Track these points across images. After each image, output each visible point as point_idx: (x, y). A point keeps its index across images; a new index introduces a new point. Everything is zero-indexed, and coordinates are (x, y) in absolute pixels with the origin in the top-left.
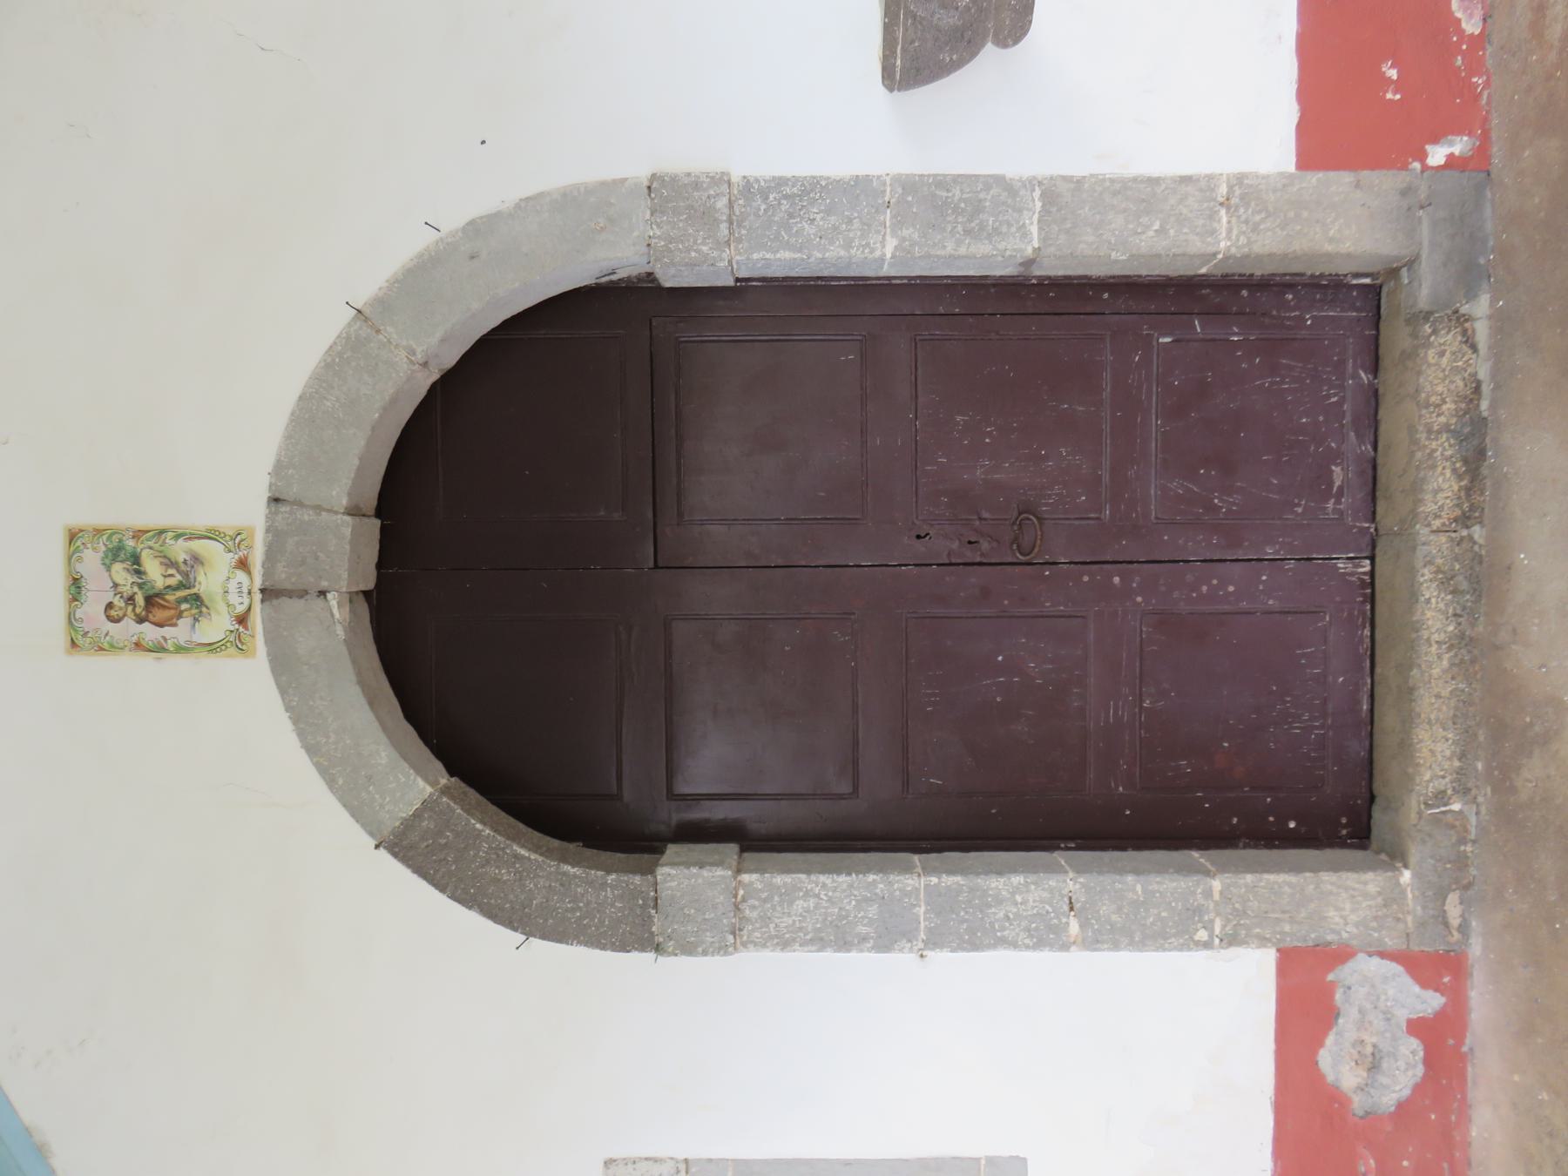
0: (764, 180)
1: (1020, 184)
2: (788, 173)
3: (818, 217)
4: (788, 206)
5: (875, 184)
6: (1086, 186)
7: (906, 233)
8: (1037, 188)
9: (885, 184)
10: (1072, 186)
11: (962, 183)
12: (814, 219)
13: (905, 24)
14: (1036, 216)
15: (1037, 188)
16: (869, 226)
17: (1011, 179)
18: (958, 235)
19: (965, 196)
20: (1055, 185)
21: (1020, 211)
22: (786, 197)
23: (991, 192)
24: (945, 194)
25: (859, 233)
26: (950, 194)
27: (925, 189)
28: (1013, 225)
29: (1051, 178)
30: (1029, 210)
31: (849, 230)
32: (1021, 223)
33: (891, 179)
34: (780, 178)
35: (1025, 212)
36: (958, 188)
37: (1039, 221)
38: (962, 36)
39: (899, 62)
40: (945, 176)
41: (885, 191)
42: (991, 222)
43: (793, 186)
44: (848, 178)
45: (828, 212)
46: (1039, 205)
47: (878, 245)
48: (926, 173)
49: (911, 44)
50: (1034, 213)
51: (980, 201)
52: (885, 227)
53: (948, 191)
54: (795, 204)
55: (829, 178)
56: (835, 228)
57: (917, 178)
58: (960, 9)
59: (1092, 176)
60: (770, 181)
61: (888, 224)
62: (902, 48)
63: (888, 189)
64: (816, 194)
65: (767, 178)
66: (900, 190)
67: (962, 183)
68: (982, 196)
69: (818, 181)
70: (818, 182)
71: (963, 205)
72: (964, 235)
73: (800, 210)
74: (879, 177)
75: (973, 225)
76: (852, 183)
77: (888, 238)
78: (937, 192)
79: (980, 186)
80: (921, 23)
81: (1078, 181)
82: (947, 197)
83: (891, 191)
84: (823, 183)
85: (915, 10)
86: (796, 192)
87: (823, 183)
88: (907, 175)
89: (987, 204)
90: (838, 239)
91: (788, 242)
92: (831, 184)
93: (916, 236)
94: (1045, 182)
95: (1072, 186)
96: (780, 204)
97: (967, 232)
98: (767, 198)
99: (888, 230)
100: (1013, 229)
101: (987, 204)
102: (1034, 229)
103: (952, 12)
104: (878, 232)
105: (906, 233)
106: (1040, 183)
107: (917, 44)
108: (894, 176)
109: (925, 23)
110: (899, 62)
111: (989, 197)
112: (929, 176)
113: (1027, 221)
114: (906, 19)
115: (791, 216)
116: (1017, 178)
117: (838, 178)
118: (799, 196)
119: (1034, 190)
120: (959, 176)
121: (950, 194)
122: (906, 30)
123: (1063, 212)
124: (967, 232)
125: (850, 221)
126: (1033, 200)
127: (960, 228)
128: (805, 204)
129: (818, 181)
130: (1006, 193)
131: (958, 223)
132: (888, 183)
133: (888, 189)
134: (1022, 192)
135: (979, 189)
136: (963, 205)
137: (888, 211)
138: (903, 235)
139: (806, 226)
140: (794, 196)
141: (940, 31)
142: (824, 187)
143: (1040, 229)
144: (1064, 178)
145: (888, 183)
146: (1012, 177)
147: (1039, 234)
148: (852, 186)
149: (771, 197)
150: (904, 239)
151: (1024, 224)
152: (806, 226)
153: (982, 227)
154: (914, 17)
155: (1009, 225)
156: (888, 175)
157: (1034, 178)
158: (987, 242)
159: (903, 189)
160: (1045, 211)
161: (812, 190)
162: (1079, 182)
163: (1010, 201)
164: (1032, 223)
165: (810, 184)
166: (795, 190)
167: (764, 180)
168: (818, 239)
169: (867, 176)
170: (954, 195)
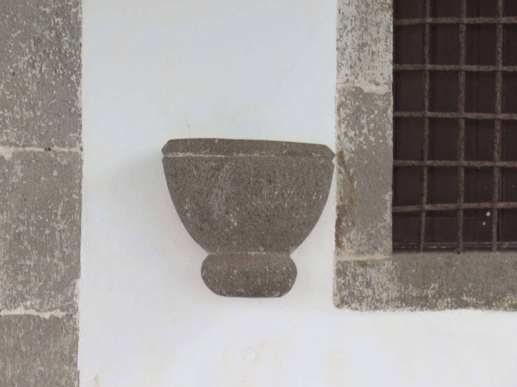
0: (78, 11)
1: (70, 295)
2: (86, 39)
3: (37, 72)
4: (48, 38)
5: (71, 135)
6: (67, 368)
7: (18, 168)
8: (64, 314)
9: (71, 146)
10: (67, 352)
11: (71, 231)
12: (34, 67)
13: (211, 159)
14: (34, 313)
15: (64, 314)
16: (26, 129)
17: (74, 284)
18: (14, 226)
19: (57, 234)
20: (67, 333)
21: (40, 295)
22: (58, 36)
23: (61, 263)
24: (59, 212)
25: (18, 117)
26: (59, 218)
27: (66, 191)
28: (24, 286)
29: (75, 329)
30: (41, 305)
31: (21, 106)
32: (27, 296)
33: (76, 153)
34: (79, 30)
35: (39, 301)
36: (66, 227)
37: (29, 316)
38: (204, 221)
39: (181, 155)
40: (80, 212)
41: (64, 146)
42: (28, 263)
43: (70, 44)
44: (79, 105)
45: (42, 83)
46: (47, 315)
47: (5, 138)
48: (83, 191)
49: (195, 166)
50: (37, 310)
51: (52, 251)
52: (24, 146)
53: (63, 216)
54: (51, 46)
55: (79, 84)
56: (24, 90)
57: (77, 181)
58: (226, 216)
59: (77, 373)
60: (76, 19)
61: (28, 149)
62: (192, 158)
63: (66, 150)
64: (62, 69)
65: (80, 16)
66: (64, 162)
67: (71, 231)
68: (57, 253)
69: (75, 72)
70: (74, 72)
71: (47, 232)
72: (15, 233)
73: (45, 52)
74: (79, 139)
75: (26, 243)
76: (73, 110)
77: (12, 149)
78: (62, 203)
79: (67, 251)
80: (213, 175)
81: (71, 359)
82: (56, 215)
83: (64, 153)
84: (73, 78)
85: (224, 169)
86: (64, 47)
87: (73, 78)
88: (80, 171)
89: (48, 259)
90: (11, 93)
91: (9, 37)
92: (73, 87)
93: (14, 180)
94: (71, 322)
95: (67, 352)
96: (51, 29)
97: (18, 237)
98: (57, 15)
99: (21, 149)
100: (20, 288)
101: (48, 259)
102: (20, 311)
103: (223, 208)
104: (19, 138)
105: (18, 168)
106: (70, 317)
107: (195, 172)
108: (80, 155)
109: (213, 179)
110: (181, 155)
111: (55, 261)
112: (80, 195)
113: (29, 303)
114: (216, 160)
115: (38, 41)
116: (76, 292)
117: (78, 94)
118: (60, 51)
119: (62, 310)
120: (79, 228)
121: (59, 218)
122: (207, 161)
123: (38, 342)
124: (18, 237)
125: (31, 107)
126: (51, 309)
127: (22, 228)
128: (51, 57)
129: (75, 72)
130: (59, 280)
131: (28, 227)
132: (72, 150)
133: (66, 150)
134: (60, 298)
135: (64, 250)
136: (47, 232)
137: (42, 150)
138: (16, 167)
139: (26, 58)
140: (60, 44)
141: (207, 197)
142: (70, 79)
143: (20, 317)
144: (75, 343)
145: (73, 150)
146: (77, 286)
147: (15, 316)
148: (70, 110)
149: (58, 20)
150: (11, 166)
151: (26, 300)
152: (26, 58)
153: (24, 253)
154: (218, 169)
155: (25, 284)
156: (82, 149)
157: (76, 311)
158: (7, 258)
159: (66, 166)
160: (40, 322)
161: (66, 65)
162: (72, 361)
163: (51, 284)
164: (26, 308)
165: (72, 63)
166: (66, 46)
167: (78, 11)
168: (12, 71)
169: (81, 126)
170: (58, 222)
